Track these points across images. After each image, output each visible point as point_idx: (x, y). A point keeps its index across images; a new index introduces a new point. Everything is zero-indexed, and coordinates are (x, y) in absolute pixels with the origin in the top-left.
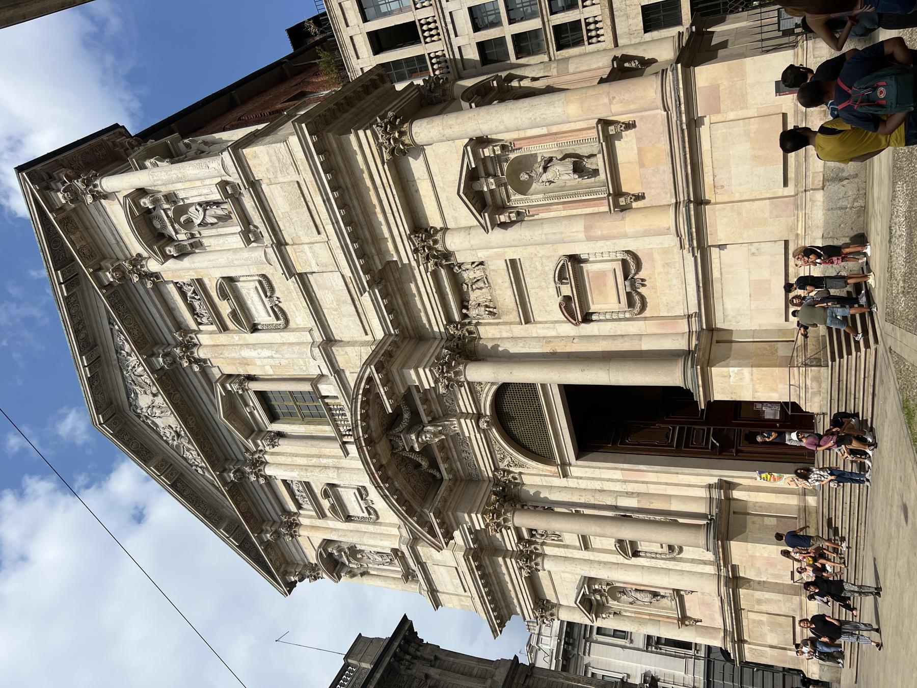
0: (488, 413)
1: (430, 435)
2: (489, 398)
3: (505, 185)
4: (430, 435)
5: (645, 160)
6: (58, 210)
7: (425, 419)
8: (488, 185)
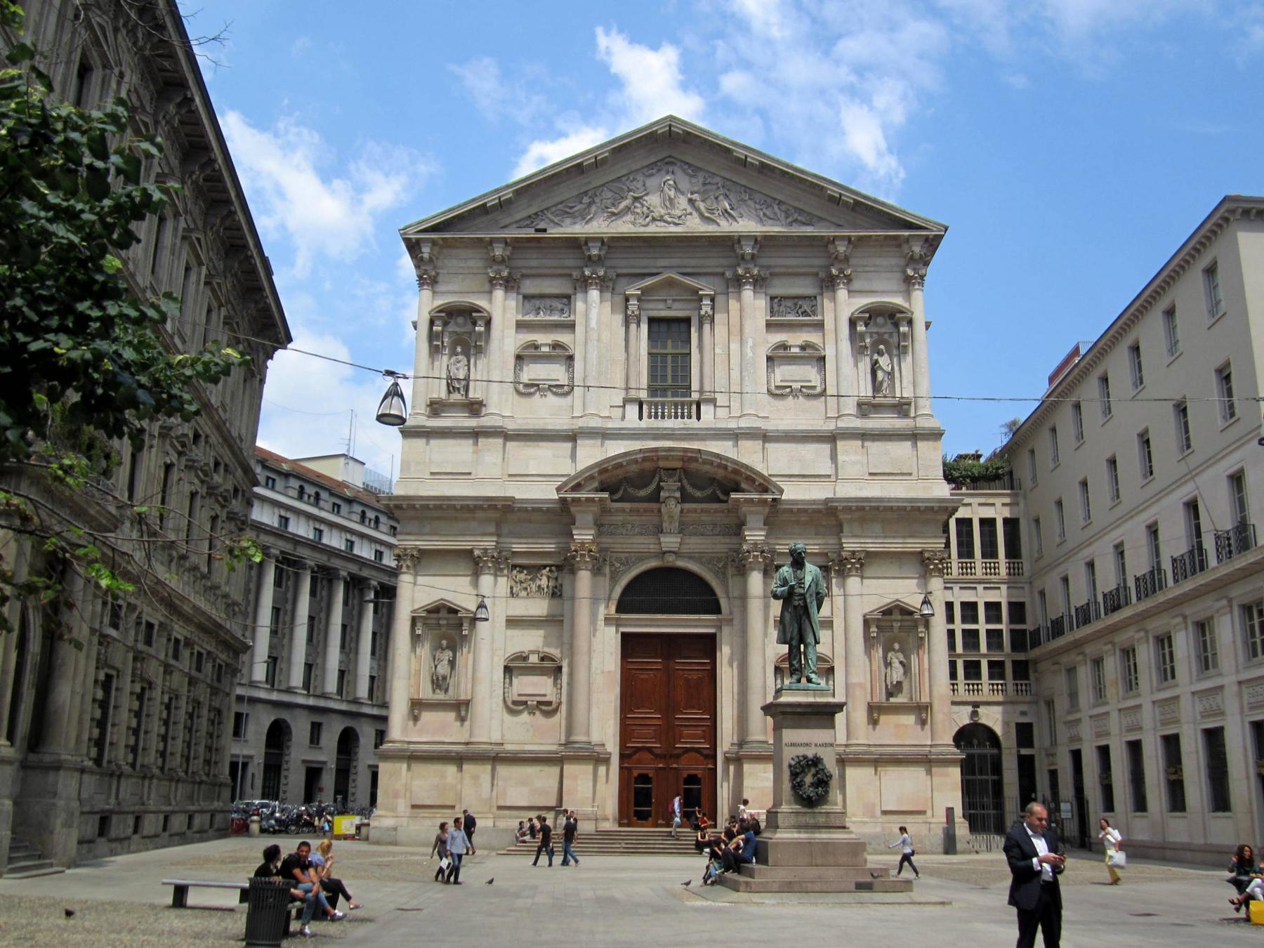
1: (673, 508)
4: (673, 508)
7: (687, 506)
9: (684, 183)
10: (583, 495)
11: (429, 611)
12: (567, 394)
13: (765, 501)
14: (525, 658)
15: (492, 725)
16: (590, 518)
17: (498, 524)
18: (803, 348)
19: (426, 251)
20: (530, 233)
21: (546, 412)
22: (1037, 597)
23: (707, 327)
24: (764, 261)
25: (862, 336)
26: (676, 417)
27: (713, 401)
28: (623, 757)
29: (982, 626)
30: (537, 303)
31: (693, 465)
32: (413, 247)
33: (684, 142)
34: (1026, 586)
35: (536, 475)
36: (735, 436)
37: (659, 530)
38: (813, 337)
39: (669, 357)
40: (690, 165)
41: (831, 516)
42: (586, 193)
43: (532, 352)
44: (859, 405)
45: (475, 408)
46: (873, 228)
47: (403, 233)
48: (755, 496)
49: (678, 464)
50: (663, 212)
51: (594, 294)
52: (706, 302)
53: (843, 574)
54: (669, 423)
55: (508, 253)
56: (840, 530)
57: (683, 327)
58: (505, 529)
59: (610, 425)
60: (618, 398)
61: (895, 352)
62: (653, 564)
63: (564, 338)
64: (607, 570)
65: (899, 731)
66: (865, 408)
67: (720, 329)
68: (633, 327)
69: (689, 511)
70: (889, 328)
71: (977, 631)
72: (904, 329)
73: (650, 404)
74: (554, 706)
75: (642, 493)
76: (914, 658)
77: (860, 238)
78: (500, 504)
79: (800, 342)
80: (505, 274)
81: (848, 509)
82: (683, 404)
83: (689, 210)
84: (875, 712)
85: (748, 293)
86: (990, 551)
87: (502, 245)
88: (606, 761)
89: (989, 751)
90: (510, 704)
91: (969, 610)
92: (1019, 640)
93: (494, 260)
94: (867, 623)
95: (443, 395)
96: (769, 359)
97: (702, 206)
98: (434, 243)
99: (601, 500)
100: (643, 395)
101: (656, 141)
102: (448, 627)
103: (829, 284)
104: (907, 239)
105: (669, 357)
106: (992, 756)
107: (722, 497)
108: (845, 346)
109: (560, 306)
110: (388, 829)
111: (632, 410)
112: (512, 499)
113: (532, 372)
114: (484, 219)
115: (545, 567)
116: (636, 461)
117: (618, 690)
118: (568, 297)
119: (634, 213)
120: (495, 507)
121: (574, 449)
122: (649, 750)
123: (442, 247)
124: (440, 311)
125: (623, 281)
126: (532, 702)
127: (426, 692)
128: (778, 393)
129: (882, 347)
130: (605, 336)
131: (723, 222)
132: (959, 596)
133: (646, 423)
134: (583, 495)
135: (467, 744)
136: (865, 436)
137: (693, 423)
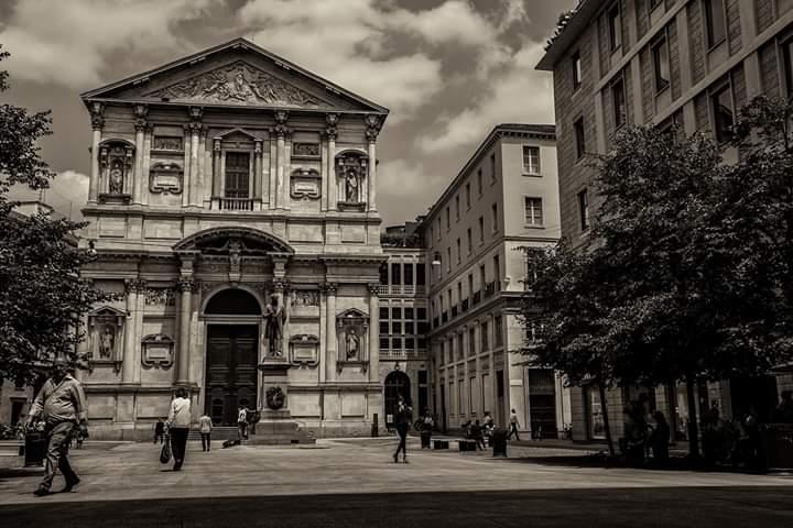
5: (353, 375)
7: (244, 257)
9: (248, 77)
12: (178, 194)
13: (284, 257)
14: (154, 338)
15: (134, 374)
16: (190, 263)
17: (139, 265)
18: (310, 172)
19: (97, 107)
20: (157, 100)
21: (166, 203)
23: (258, 159)
24: (291, 124)
25: (341, 168)
27: (261, 201)
28: (206, 390)
29: (390, 320)
30: (163, 141)
31: (247, 236)
32: (89, 105)
35: (162, 237)
36: (271, 219)
37: (229, 270)
38: (316, 167)
41: (320, 264)
42: (192, 79)
43: (159, 168)
45: (126, 199)
46: (349, 109)
47: (83, 95)
49: (239, 235)
50: (236, 92)
52: (258, 145)
53: (327, 294)
54: (235, 212)
56: (325, 269)
57: (246, 158)
58: (143, 268)
59: (203, 212)
60: (208, 198)
62: (226, 287)
63: (178, 162)
64: (200, 291)
66: (341, 206)
67: (266, 162)
68: (217, 158)
70: (356, 163)
75: (219, 250)
76: (361, 339)
78: (140, 254)
80: (144, 124)
84: (340, 365)
85: (281, 142)
88: (198, 392)
92: (423, 328)
93: (137, 115)
94: (337, 320)
95: (107, 192)
96: (292, 178)
97: (257, 90)
98: (102, 103)
99: (197, 254)
100: (222, 195)
102: (113, 323)
103: (325, 138)
108: (333, 173)
111: (215, 205)
112: (148, 252)
114: (131, 92)
115: (165, 288)
117: (205, 355)
118: (181, 138)
120: (136, 256)
121: (182, 225)
122: (221, 386)
125: (212, 130)
126: (157, 361)
128: (296, 197)
130: (202, 161)
131: (270, 101)
134: (187, 252)
136: (340, 221)
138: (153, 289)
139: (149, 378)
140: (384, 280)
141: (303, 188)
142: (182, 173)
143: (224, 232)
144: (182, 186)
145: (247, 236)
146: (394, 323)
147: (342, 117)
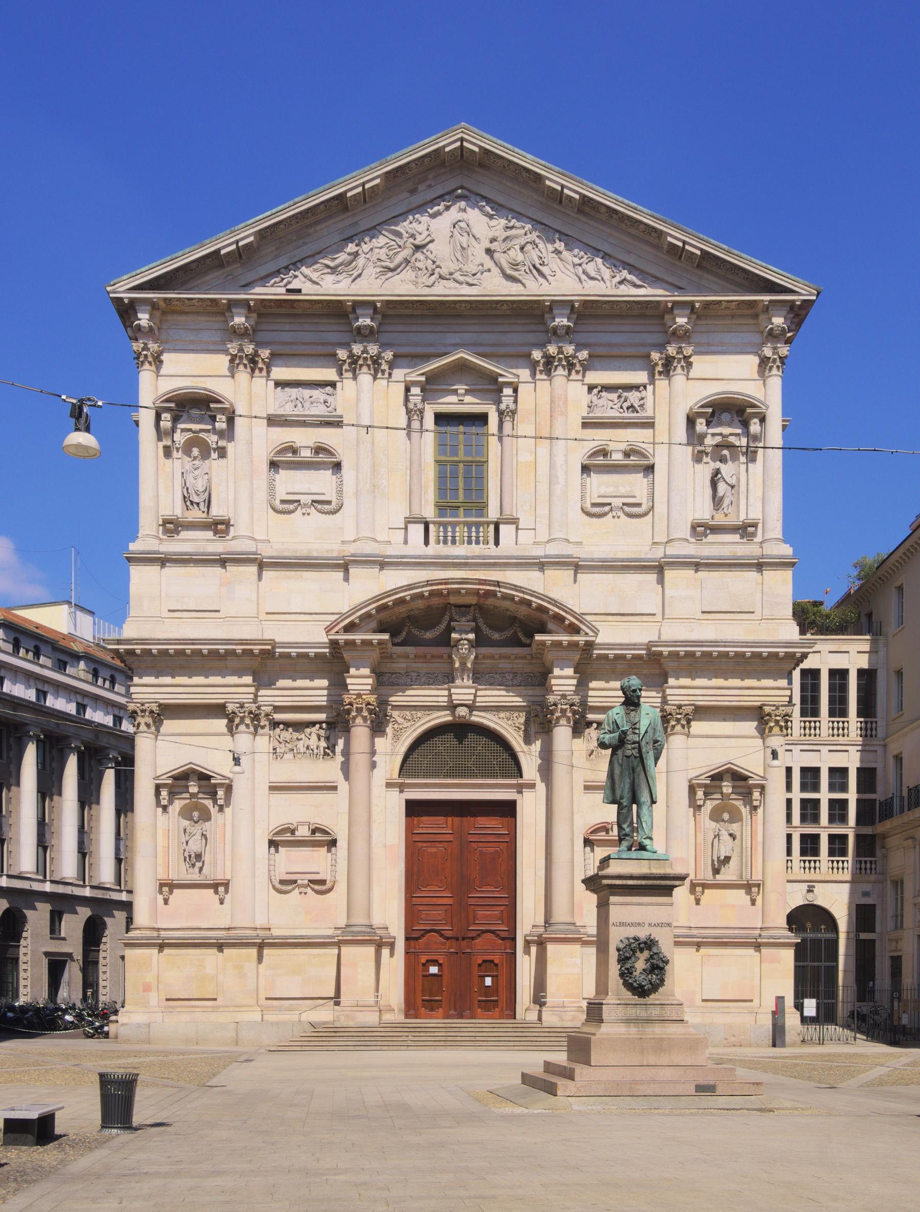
0: (473, 718)
2: (492, 725)
3: (722, 800)
6: (767, 309)
8: (727, 787)
10: (358, 637)
11: (175, 778)
13: (575, 644)
15: (257, 905)
21: (306, 534)
22: (891, 761)
26: (470, 543)
28: (407, 939)
33: (481, 165)
34: (880, 749)
39: (461, 465)
40: (489, 201)
44: (693, 528)
45: (220, 527)
46: (724, 291)
48: (565, 638)
49: (472, 600)
51: (365, 378)
54: (461, 550)
55: (253, 323)
59: (390, 551)
61: (743, 459)
63: (326, 436)
65: (727, 909)
66: (701, 529)
69: (484, 657)
71: (818, 801)
72: (755, 427)
73: (434, 523)
74: (329, 885)
77: (707, 305)
79: (623, 446)
81: (674, 655)
82: (478, 525)
83: (489, 263)
86: (838, 708)
87: (244, 311)
88: (392, 945)
89: (823, 935)
90: (278, 886)
91: (810, 776)
98: (153, 306)
99: (381, 642)
100: (429, 512)
101: (443, 164)
104: (767, 309)
105: (461, 465)
106: (827, 940)
107: (524, 640)
109: (323, 397)
110: (139, 1026)
111: (417, 531)
113: (291, 482)
114: (214, 276)
116: (421, 596)
119: (415, 268)
123: (164, 313)
124: (167, 401)
126: (303, 880)
127: (180, 872)
129: (725, 452)
132: (800, 760)
133: (434, 549)
135: (229, 929)
136: (697, 566)
137: (490, 550)
138: (287, 725)
139: (290, 915)
140: (810, 707)
141: (610, 490)
142: (337, 466)
143: (438, 593)
144: (340, 492)
145: (490, 601)
146: (832, 802)
147: (697, 313)
